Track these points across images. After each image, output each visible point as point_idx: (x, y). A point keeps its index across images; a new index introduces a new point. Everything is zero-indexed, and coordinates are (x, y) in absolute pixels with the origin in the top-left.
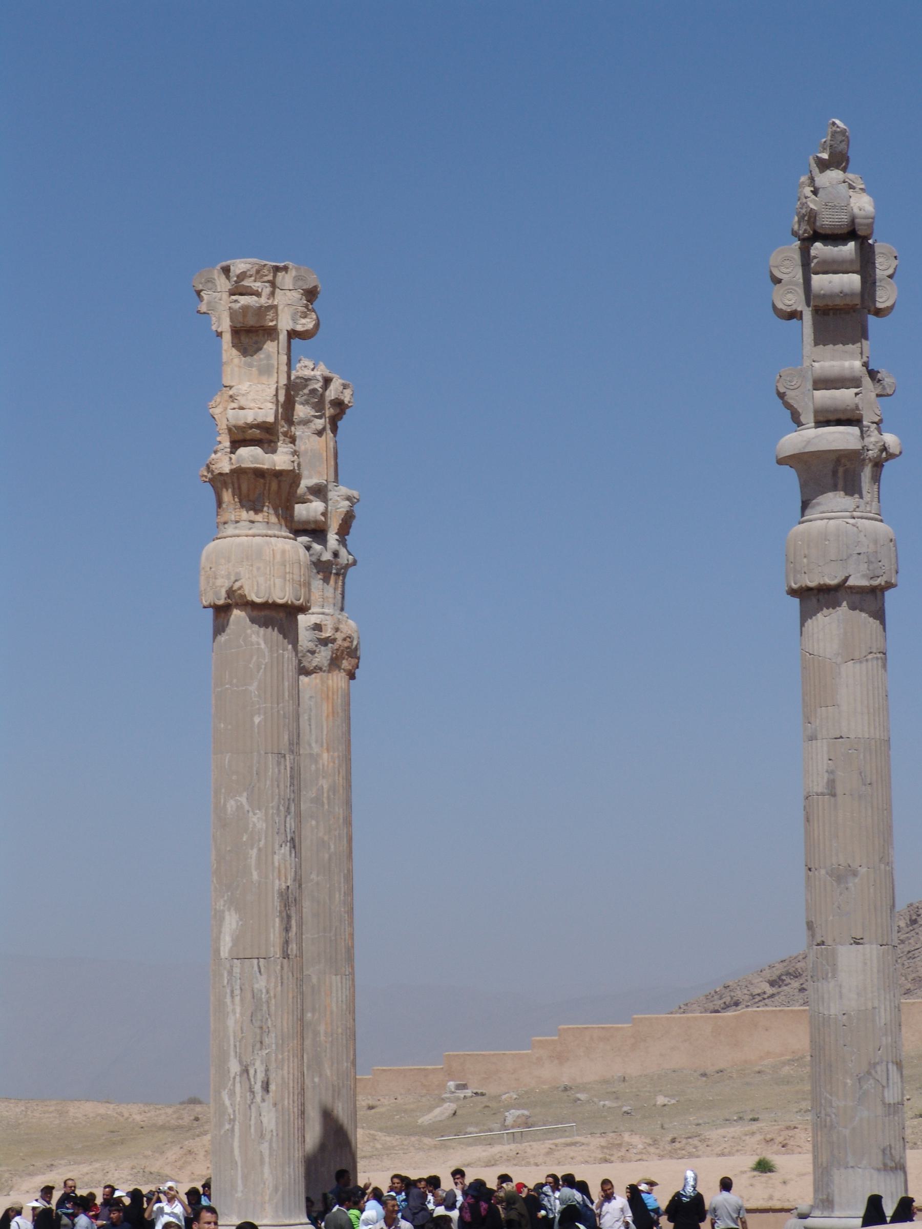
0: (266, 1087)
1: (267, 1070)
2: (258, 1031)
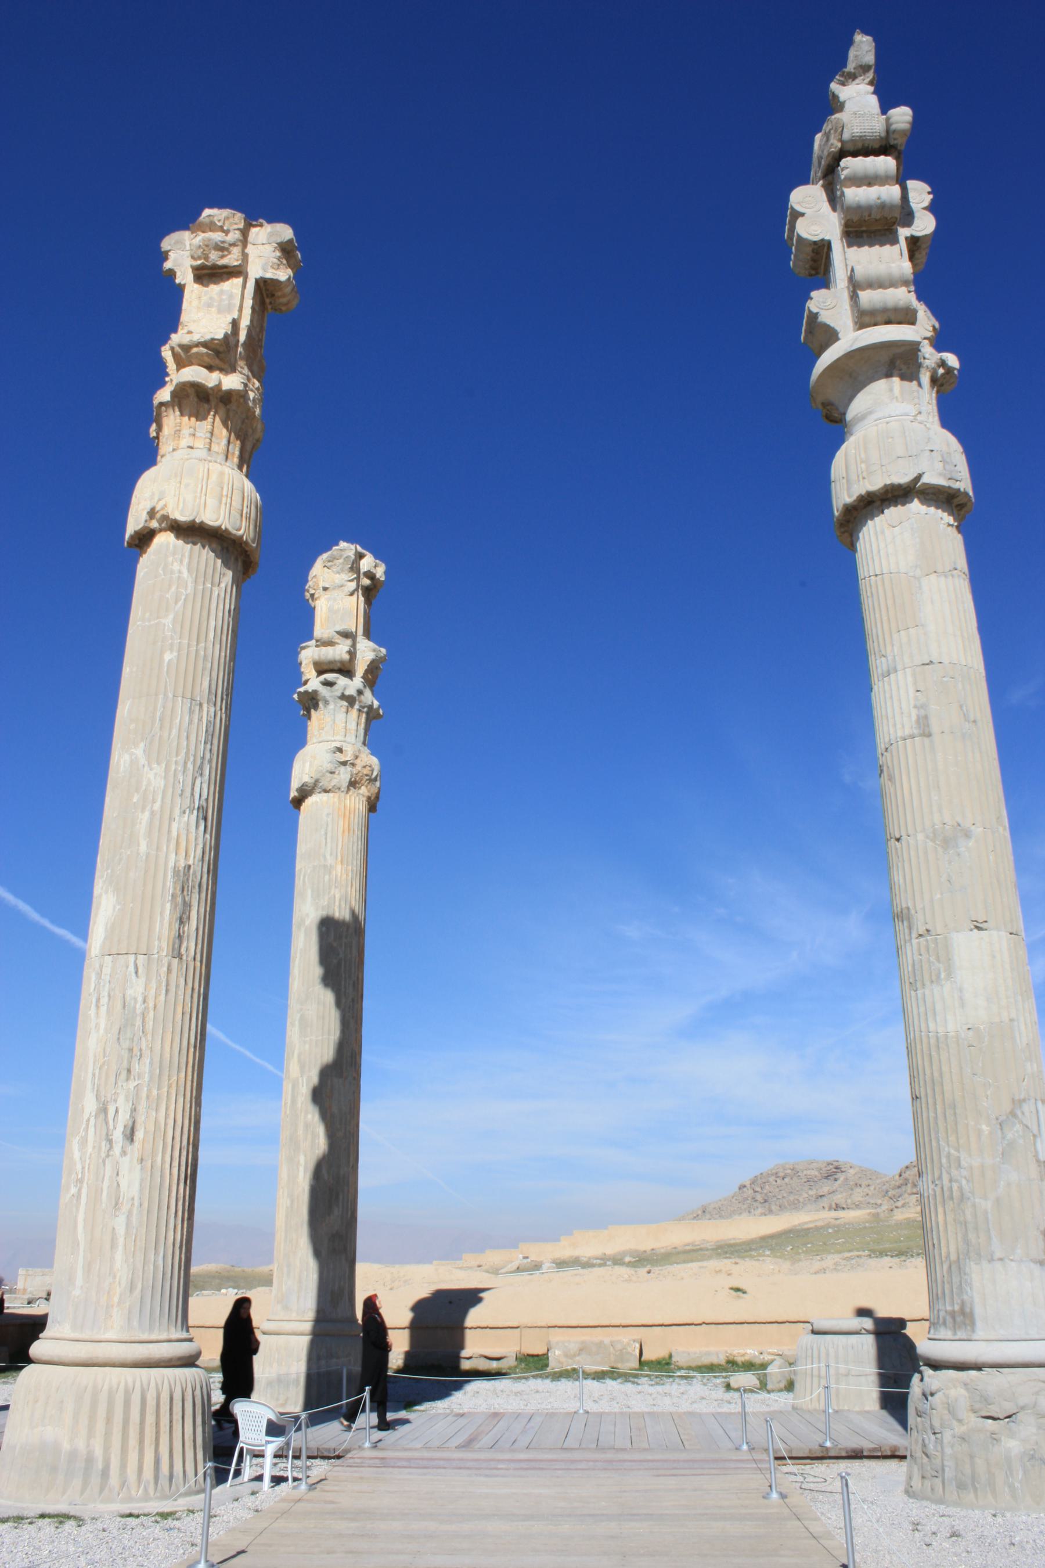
0: (130, 1135)
1: (134, 1110)
2: (125, 1054)
